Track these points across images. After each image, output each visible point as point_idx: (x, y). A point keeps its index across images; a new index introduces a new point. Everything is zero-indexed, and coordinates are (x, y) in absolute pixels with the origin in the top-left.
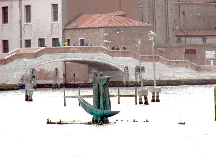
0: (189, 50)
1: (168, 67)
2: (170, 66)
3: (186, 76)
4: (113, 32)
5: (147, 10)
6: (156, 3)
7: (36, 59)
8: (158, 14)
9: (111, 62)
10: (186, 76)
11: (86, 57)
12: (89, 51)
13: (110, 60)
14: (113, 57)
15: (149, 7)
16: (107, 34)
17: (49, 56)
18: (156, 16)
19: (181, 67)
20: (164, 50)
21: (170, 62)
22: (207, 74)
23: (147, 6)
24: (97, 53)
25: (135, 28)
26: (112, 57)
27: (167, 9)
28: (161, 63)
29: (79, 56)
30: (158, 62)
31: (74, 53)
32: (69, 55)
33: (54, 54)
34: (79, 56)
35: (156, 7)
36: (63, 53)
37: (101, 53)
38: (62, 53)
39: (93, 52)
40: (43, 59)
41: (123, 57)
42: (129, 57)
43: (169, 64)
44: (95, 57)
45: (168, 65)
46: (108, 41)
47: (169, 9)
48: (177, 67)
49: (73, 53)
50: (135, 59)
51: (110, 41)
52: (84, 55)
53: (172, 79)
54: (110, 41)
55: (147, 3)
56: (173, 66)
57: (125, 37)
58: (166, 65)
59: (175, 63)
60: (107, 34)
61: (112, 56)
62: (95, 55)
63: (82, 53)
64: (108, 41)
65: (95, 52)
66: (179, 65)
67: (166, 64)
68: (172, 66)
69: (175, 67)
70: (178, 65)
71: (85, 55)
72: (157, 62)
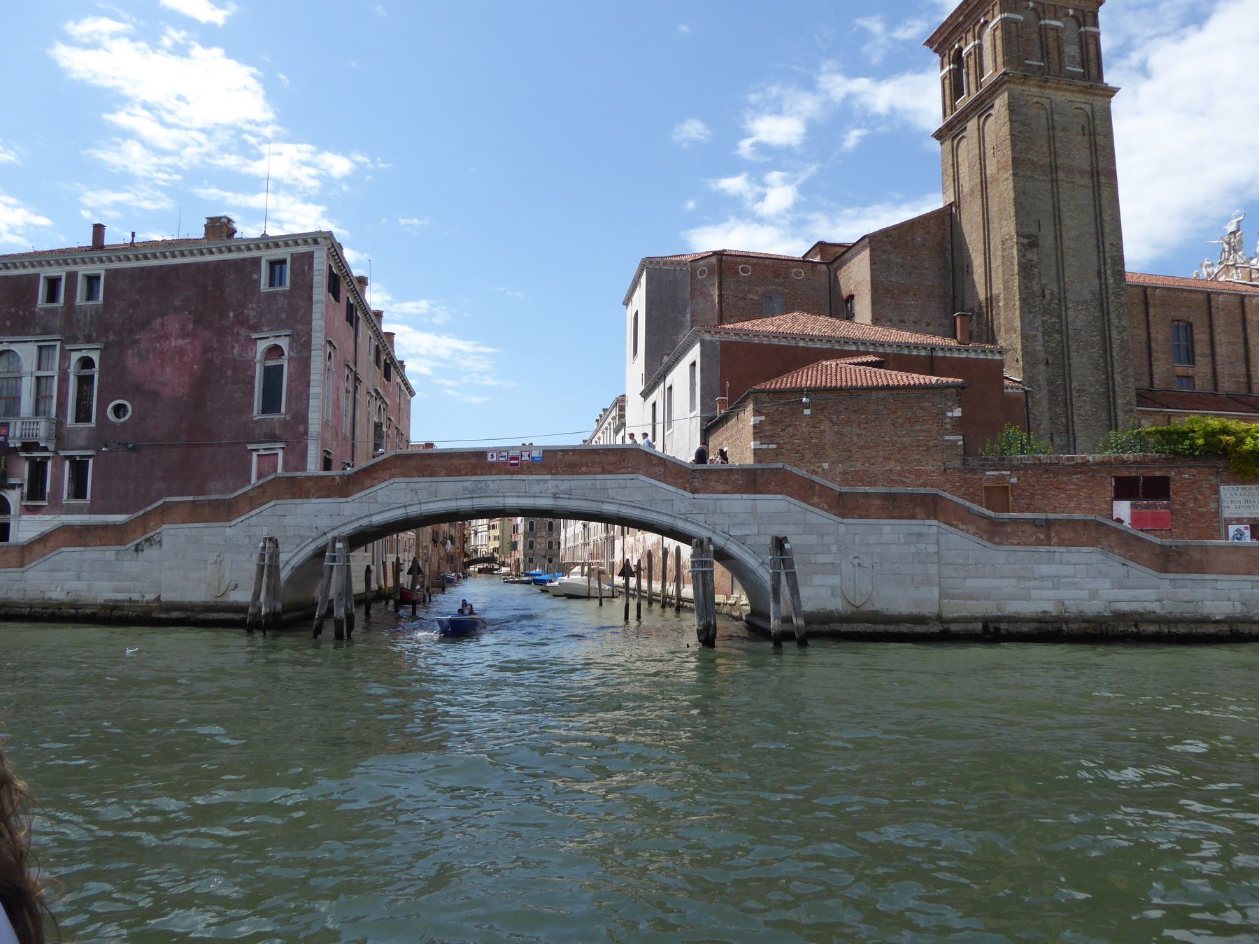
0: (1136, 479)
1: (994, 546)
2: (1000, 544)
3: (1094, 595)
4: (787, 408)
5: (1045, 402)
6: (1075, 384)
7: (349, 499)
8: (1082, 412)
9: (686, 520)
10: (1094, 595)
11: (569, 494)
12: (584, 469)
13: (683, 511)
14: (696, 496)
15: (1052, 393)
16: (763, 418)
17: (404, 486)
18: (1076, 418)
19: (1063, 549)
20: (1014, 480)
21: (1003, 524)
22: (1220, 585)
23: (1045, 392)
24: (619, 476)
25: (882, 394)
26: (691, 495)
27: (1115, 403)
28: (952, 529)
29: (536, 489)
30: (935, 522)
31: (515, 477)
32: (492, 485)
33: (429, 479)
34: (536, 489)
35: (1074, 393)
36: (466, 474)
37: (641, 477)
38: (461, 475)
39: (602, 473)
40: (379, 499)
41: (745, 496)
42: (781, 497)
43: (995, 532)
44: (612, 493)
45: (990, 540)
46: (765, 446)
47: (1119, 401)
48: (1042, 549)
49: (508, 477)
50: (809, 507)
51: (774, 446)
52: (558, 483)
53: (1014, 607)
54: (774, 446)
55: (1043, 383)
56: (1018, 544)
57: (836, 428)
58: (980, 540)
59: (1029, 530)
60: (763, 418)
61: (694, 491)
62: (609, 484)
63: (549, 477)
64: (765, 446)
65: (610, 472)
66: (1055, 540)
67: (975, 534)
68: (1012, 544)
69: (1032, 548)
70: (1049, 538)
71: (564, 486)
72: (928, 522)
